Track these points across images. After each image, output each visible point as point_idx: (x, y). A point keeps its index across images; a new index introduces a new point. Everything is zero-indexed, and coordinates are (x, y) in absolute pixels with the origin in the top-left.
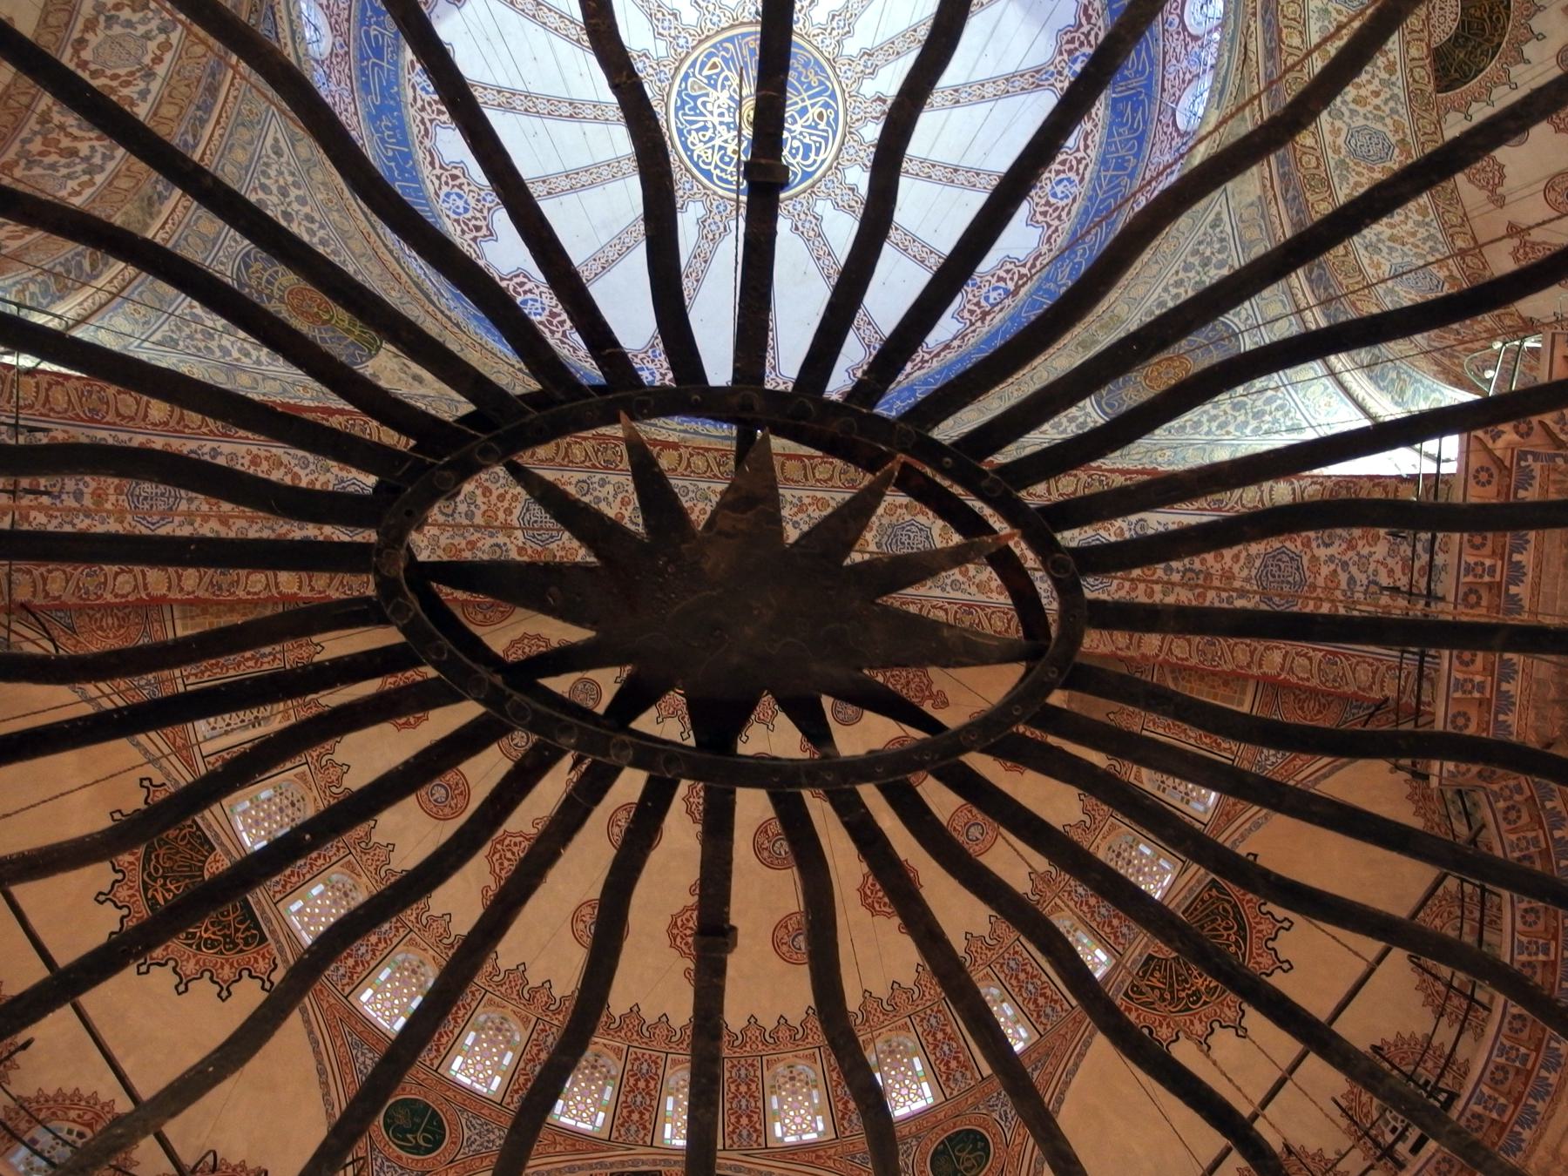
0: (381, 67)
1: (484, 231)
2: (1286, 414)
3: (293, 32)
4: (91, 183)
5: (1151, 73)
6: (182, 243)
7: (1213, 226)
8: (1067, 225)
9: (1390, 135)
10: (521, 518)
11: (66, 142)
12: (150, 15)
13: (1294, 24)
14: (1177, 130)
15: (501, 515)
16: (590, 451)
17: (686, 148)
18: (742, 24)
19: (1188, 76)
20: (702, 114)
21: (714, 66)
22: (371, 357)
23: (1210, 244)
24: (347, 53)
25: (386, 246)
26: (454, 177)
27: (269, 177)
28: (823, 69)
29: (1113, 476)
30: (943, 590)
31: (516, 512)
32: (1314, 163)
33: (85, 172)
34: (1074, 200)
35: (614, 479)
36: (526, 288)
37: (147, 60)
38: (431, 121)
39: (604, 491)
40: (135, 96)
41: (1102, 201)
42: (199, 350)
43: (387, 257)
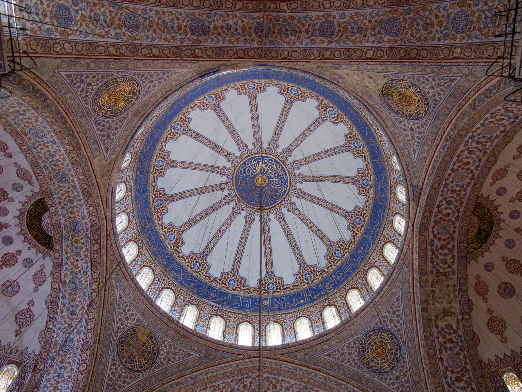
1: (348, 137)
2: (72, 82)
3: (408, 189)
4: (473, 132)
5: (136, 201)
6: (446, 116)
8: (157, 152)
9: (56, 182)
10: (335, 29)
11: (479, 146)
13: (93, 214)
14: (125, 183)
15: (342, 29)
17: (284, 170)
19: (124, 200)
21: (276, 196)
22: (386, 84)
23: (108, 143)
24: (391, 188)
25: (380, 124)
26: (358, 153)
30: (185, 12)
31: (336, 31)
32: (78, 170)
33: (475, 136)
34: (156, 160)
35: (303, 46)
36: (334, 119)
37: (453, 175)
38: (365, 170)
41: (146, 160)
42: (442, 79)
43: (380, 120)
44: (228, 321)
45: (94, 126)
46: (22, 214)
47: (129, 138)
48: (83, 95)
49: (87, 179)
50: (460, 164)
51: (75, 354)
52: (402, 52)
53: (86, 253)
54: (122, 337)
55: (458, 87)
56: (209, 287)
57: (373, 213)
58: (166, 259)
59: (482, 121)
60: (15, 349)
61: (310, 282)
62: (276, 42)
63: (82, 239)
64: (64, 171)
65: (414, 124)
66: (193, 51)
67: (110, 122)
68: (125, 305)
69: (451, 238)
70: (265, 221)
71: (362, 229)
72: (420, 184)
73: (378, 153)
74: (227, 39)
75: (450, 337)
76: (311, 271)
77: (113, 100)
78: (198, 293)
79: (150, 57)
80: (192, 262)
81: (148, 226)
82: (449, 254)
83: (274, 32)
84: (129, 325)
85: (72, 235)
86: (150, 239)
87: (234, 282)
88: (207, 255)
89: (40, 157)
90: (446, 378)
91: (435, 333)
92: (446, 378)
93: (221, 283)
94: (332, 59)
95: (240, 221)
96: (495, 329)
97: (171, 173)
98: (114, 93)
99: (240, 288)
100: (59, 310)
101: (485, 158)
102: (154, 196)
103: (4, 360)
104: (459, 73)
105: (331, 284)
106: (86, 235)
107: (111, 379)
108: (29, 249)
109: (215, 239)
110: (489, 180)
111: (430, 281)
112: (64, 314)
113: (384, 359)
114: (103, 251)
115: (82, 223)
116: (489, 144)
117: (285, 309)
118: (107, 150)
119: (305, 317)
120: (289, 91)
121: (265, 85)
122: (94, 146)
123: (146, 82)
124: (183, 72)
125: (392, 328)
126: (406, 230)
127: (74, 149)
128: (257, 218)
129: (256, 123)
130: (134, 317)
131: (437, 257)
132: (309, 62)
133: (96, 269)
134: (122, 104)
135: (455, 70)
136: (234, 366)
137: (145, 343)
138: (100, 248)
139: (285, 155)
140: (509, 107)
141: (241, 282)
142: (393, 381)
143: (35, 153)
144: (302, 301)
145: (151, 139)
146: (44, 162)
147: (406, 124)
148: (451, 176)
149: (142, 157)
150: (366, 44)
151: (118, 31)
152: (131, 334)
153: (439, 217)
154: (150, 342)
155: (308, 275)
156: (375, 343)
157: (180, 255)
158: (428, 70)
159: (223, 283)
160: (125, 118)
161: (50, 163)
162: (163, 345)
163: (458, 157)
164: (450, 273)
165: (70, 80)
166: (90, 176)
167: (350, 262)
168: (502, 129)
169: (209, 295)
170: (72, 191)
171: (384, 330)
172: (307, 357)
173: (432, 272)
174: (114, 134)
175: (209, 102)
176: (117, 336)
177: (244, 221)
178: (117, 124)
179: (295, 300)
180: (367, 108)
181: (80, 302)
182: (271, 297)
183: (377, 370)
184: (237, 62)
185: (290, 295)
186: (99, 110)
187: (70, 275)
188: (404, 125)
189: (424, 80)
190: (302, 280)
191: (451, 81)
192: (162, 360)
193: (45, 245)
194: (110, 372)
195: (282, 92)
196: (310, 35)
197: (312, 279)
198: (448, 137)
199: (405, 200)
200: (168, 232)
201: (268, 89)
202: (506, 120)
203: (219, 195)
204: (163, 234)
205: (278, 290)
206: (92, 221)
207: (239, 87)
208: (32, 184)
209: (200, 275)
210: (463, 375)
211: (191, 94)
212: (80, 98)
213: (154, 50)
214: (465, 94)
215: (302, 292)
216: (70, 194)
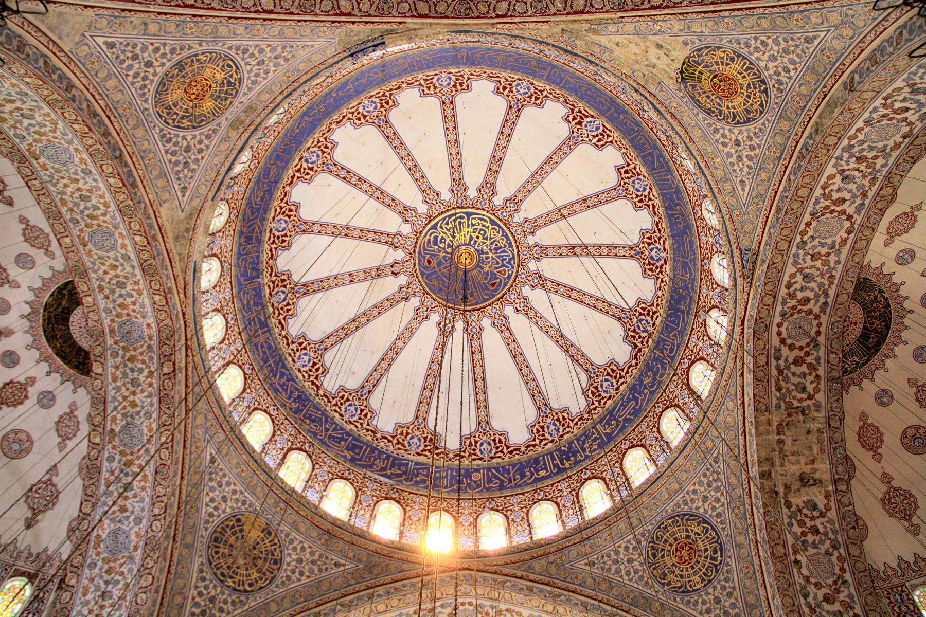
0: (683, 257)
1: (623, 171)
2: (117, 57)
3: (732, 256)
4: (850, 139)
6: (799, 112)
7: (185, 188)
8: (276, 203)
9: (93, 249)
11: (862, 167)
12: (810, 252)
17: (506, 236)
18: (479, 309)
20: (498, 257)
21: (493, 285)
22: (688, 57)
23: (185, 177)
24: (702, 261)
25: (680, 136)
26: (641, 201)
27: (748, 166)
29: (218, 7)
32: (132, 224)
33: (853, 146)
34: (274, 219)
36: (597, 139)
37: (814, 223)
38: (655, 232)
40: (822, 200)
42: (792, 39)
43: (678, 129)
44: (408, 508)
45: (160, 143)
46: (34, 311)
47: (224, 169)
48: (138, 85)
49: (148, 243)
50: (827, 203)
51: (131, 558)
54: (215, 531)
55: (822, 50)
56: (373, 449)
57: (669, 309)
58: (295, 399)
60: (26, 551)
61: (557, 439)
64: (107, 228)
65: (740, 132)
67: (189, 138)
68: (221, 473)
69: (812, 345)
70: (474, 330)
72: (755, 244)
73: (678, 198)
75: (813, 523)
77: (193, 97)
78: (352, 460)
79: (257, 12)
80: (341, 404)
81: (262, 339)
82: (810, 374)
84: (229, 510)
85: (123, 348)
87: (419, 440)
88: (369, 392)
91: (785, 517)
92: (806, 596)
93: (395, 441)
95: (429, 332)
97: (301, 242)
98: (193, 84)
100: (103, 482)
101: (874, 189)
102: (272, 285)
103: (6, 570)
105: (594, 440)
106: (149, 347)
107: (197, 605)
108: (48, 374)
109: (384, 365)
111: (775, 424)
113: (693, 568)
114: (181, 376)
116: (880, 162)
117: (511, 487)
118: (184, 189)
119: (548, 500)
120: (514, 89)
121: (469, 78)
122: (160, 183)
124: (318, 45)
125: (706, 511)
126: (730, 334)
127: (124, 185)
128: (459, 325)
129: (454, 150)
131: (787, 380)
132: (547, 22)
133: (168, 408)
134: (209, 104)
135: (815, 18)
137: (258, 543)
138: (174, 370)
139: (508, 210)
142: (708, 605)
143: (55, 194)
144: (543, 473)
145: (264, 178)
146: (72, 210)
147: (727, 132)
149: (249, 212)
152: (233, 527)
153: (790, 305)
154: (267, 541)
155: (552, 427)
156: (676, 539)
157: (321, 393)
158: (765, 23)
159: (398, 443)
160: (215, 131)
161: (82, 212)
162: (291, 547)
164: (813, 408)
165: (113, 53)
166: (154, 237)
167: (629, 400)
169: (373, 464)
170: (122, 265)
171: (692, 516)
172: (553, 569)
173: (778, 407)
174: (196, 161)
175: (369, 112)
176: (206, 529)
177: (435, 331)
178: (200, 142)
180: (655, 107)
182: (486, 466)
183: (680, 587)
184: (417, 27)
185: (521, 463)
186: (168, 114)
187: (122, 420)
188: (724, 136)
189: (759, 45)
190: (543, 435)
191: (808, 40)
192: (289, 573)
194: (196, 592)
197: (561, 433)
198: (804, 151)
199: (727, 281)
200: (298, 350)
203: (390, 285)
204: (290, 355)
205: (500, 454)
206: (159, 322)
207: (422, 82)
208: (52, 256)
209: (357, 427)
210: (838, 591)
211: (334, 95)
212: (133, 90)
214: (835, 63)
215: (543, 456)
216: (119, 271)
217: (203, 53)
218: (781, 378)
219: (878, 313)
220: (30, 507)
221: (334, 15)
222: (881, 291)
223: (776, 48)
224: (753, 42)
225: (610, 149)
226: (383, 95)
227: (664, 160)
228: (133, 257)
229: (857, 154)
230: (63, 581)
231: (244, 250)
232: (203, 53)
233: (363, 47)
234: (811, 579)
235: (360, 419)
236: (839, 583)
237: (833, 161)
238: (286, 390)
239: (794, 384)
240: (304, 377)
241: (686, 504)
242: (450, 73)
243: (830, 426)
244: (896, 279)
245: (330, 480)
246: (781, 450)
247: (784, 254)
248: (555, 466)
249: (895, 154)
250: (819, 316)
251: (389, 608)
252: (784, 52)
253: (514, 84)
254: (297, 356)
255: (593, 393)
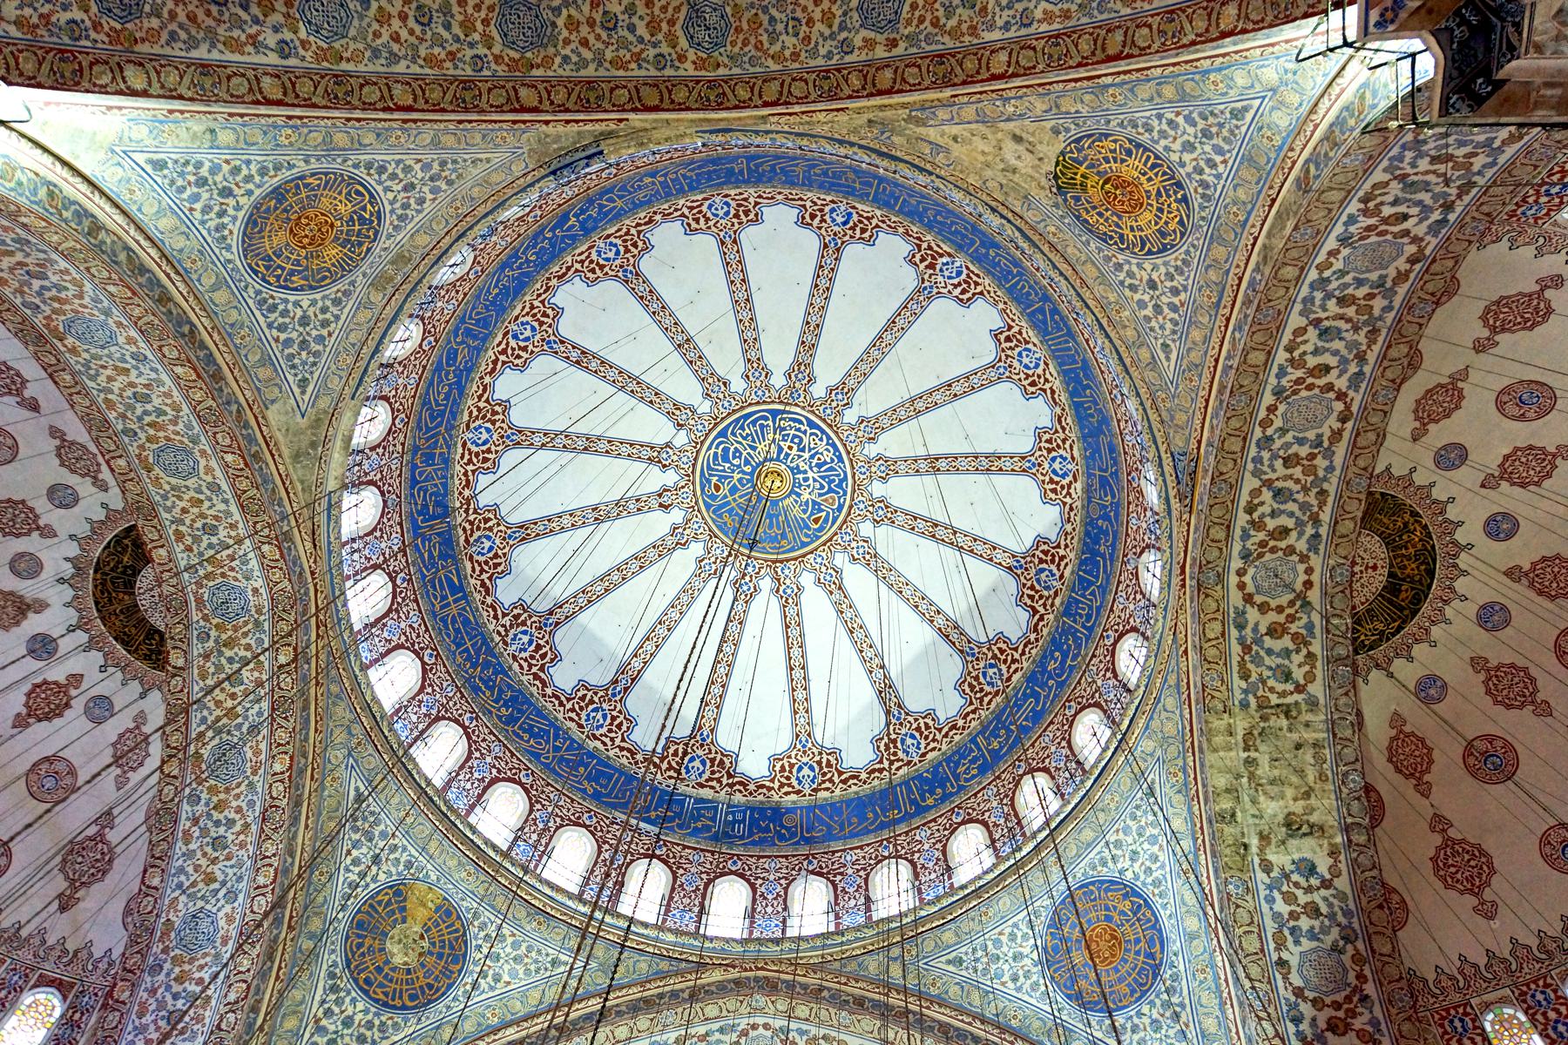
0: (1101, 470)
1: (1002, 338)
2: (173, 182)
3: (1161, 465)
6: (1239, 230)
8: (470, 402)
9: (162, 474)
11: (1350, 311)
12: (1281, 453)
14: (379, 488)
16: (844, 86)
17: (834, 445)
21: (816, 521)
22: (1063, 153)
23: (304, 363)
26: (1033, 384)
28: (719, 527)
33: (1328, 280)
35: (820, 62)
37: (1282, 408)
39: (827, 48)
40: (1290, 370)
43: (1063, 267)
44: (681, 871)
45: (257, 313)
48: (212, 224)
49: (246, 464)
50: (1299, 373)
52: (1085, 46)
53: (256, 674)
56: (631, 778)
59: (1339, 229)
61: (916, 759)
62: (746, 59)
63: (245, 635)
66: (512, 93)
67: (305, 304)
69: (1298, 603)
71: (1058, 601)
73: (1087, 377)
74: (609, 55)
76: (918, 729)
77: (306, 241)
78: (596, 796)
79: (386, 109)
80: (581, 708)
83: (738, 30)
84: (382, 877)
86: (458, 646)
87: (703, 763)
88: (626, 689)
89: (110, 405)
90: (1297, 1020)
91: (1261, 887)
93: (665, 766)
94: (900, 91)
96: (1459, 876)
99: (719, 781)
101: (1376, 348)
104: (1252, 86)
105: (973, 761)
106: (257, 624)
110: (1401, 420)
112: (193, 846)
113: (1116, 970)
115: (243, 592)
116: (1378, 304)
118: (303, 383)
120: (827, 217)
121: (757, 204)
122: (264, 373)
123: (395, 188)
124: (497, 157)
125: (1137, 877)
127: (199, 376)
128: (766, 584)
129: (745, 315)
130: (397, 855)
131: (1258, 661)
134: (332, 252)
136: (686, 995)
140: (1409, 170)
141: (722, 762)
146: (123, 416)
147: (1134, 268)
148: (1278, 413)
150: (989, 36)
151: (288, 36)
152: (389, 903)
153: (1256, 540)
155: (909, 741)
157: (549, 691)
158: (1169, 91)
160: (347, 293)
161: (140, 419)
163: (1289, 349)
164: (1304, 707)
168: (1411, 249)
170: (210, 499)
173: (1245, 705)
175: (607, 260)
178: (324, 310)
179: (876, 814)
181: (239, 810)
188: (1130, 274)
189: (1165, 127)
191: (1237, 114)
193: (147, 658)
195: (808, 219)
196: (835, 28)
201: (769, 213)
202: (1415, 220)
204: (499, 633)
206: (271, 585)
207: (686, 211)
208: (104, 488)
209: (605, 744)
210: (1352, 1014)
213: (398, 90)
217: (313, 175)
218: (1247, 658)
219: (1412, 550)
220: (67, 878)
221: (511, 111)
222: (1414, 514)
223: (1191, 130)
224: (1155, 123)
225: (980, 303)
226: (627, 233)
227: (1062, 319)
228: (224, 486)
229: (1337, 293)
230: (110, 994)
231: (421, 474)
232: (313, 175)
233: (568, 160)
234: (1307, 993)
235: (610, 731)
236: (1355, 999)
237: (1298, 307)
238: (491, 689)
239: (1270, 668)
240: (521, 667)
241: (1104, 864)
242: (727, 196)
243: (1335, 735)
244: (1436, 493)
245: (558, 828)
246: (1252, 776)
247: (1237, 460)
248: (913, 802)
249: (1402, 290)
250: (1308, 557)
251: (635, 1033)
252: (1204, 135)
253: (827, 209)
254: (511, 635)
255: (969, 685)
